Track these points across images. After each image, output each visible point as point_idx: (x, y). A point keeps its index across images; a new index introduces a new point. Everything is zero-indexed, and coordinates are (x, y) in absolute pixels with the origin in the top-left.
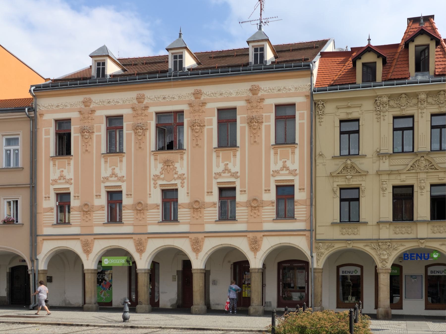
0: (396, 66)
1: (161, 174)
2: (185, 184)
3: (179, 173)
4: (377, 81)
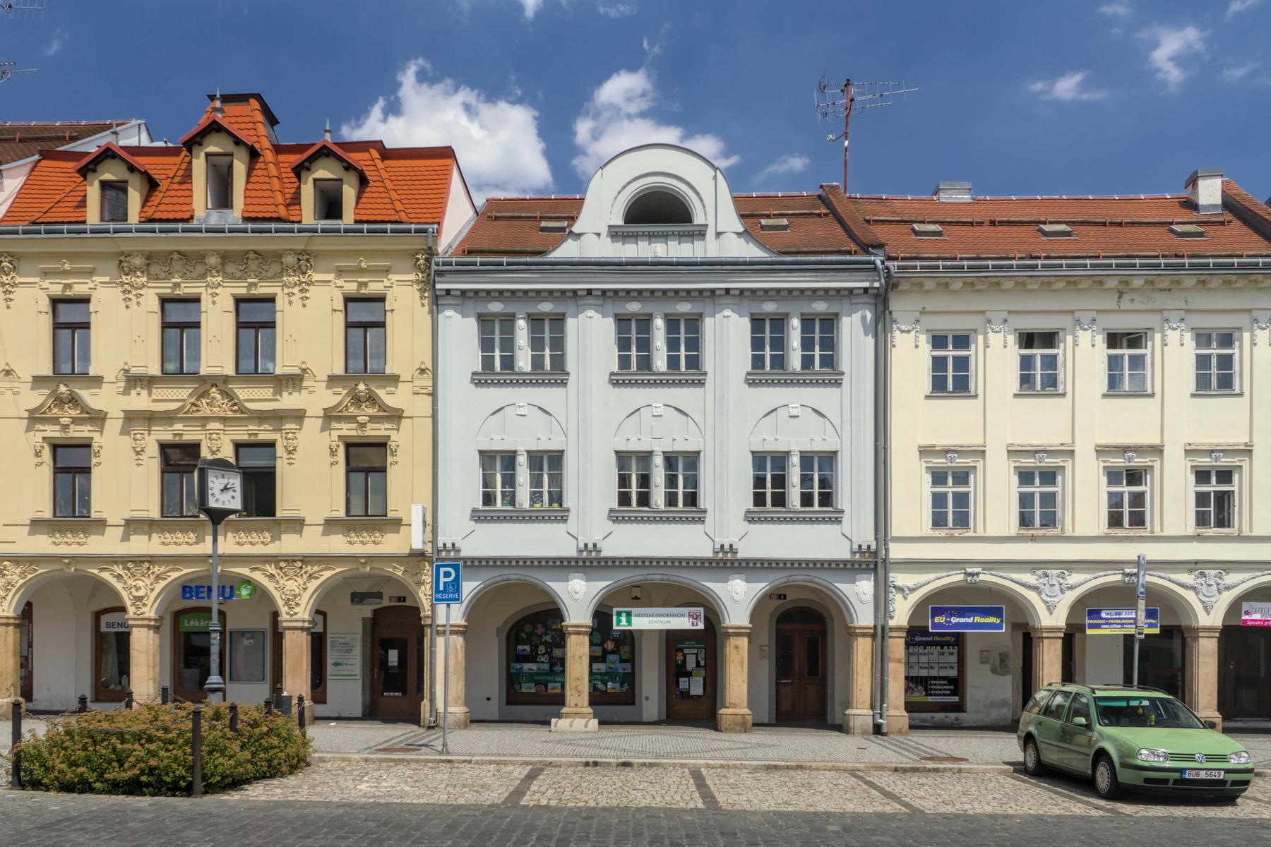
0: (169, 193)
4: (129, 222)
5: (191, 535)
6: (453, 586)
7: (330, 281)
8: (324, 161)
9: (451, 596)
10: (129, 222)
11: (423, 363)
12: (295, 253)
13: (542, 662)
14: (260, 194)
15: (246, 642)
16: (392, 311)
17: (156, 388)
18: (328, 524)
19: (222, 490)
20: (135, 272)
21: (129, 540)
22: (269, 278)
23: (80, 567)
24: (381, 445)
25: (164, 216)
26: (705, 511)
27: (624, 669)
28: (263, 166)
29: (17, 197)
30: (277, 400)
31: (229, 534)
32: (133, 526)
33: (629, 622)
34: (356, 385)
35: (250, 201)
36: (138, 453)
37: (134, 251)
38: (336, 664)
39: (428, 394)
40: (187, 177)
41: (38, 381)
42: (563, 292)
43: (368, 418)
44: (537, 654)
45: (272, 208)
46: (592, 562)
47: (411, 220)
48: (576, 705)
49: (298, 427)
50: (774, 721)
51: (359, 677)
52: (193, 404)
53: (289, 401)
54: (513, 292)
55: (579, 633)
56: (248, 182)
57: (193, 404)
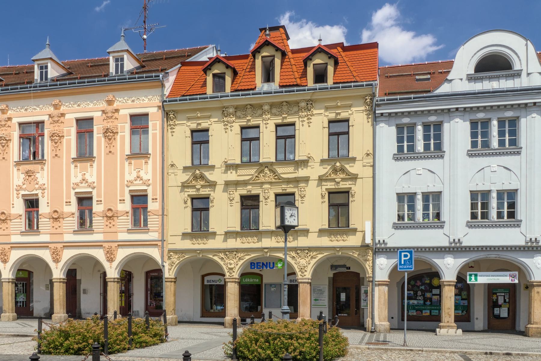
0: (244, 77)
1: (24, 185)
2: (46, 194)
3: (39, 183)
4: (226, 92)
5: (255, 238)
6: (409, 262)
7: (322, 114)
8: (318, 55)
9: (408, 267)
10: (226, 92)
12: (305, 101)
13: (420, 300)
14: (287, 74)
15: (273, 289)
16: (353, 126)
17: (239, 170)
18: (321, 232)
19: (290, 216)
20: (230, 115)
21: (226, 241)
22: (292, 114)
23: (204, 254)
24: (347, 192)
25: (243, 88)
26: (521, 221)
27: (464, 304)
28: (288, 60)
29: (173, 85)
30: (296, 173)
31: (273, 238)
32: (228, 235)
33: (476, 280)
34: (335, 163)
35: (282, 77)
36: (231, 200)
37: (230, 106)
38: (316, 300)
39: (371, 166)
40: (253, 68)
41: (186, 169)
42: (443, 110)
43: (341, 179)
44: (417, 296)
45: (294, 80)
46: (458, 249)
47: (362, 80)
48: (448, 322)
49: (306, 185)
51: (327, 306)
52: (257, 176)
53: (302, 173)
54: (416, 112)
55: (450, 285)
56: (281, 69)
57: (257, 176)
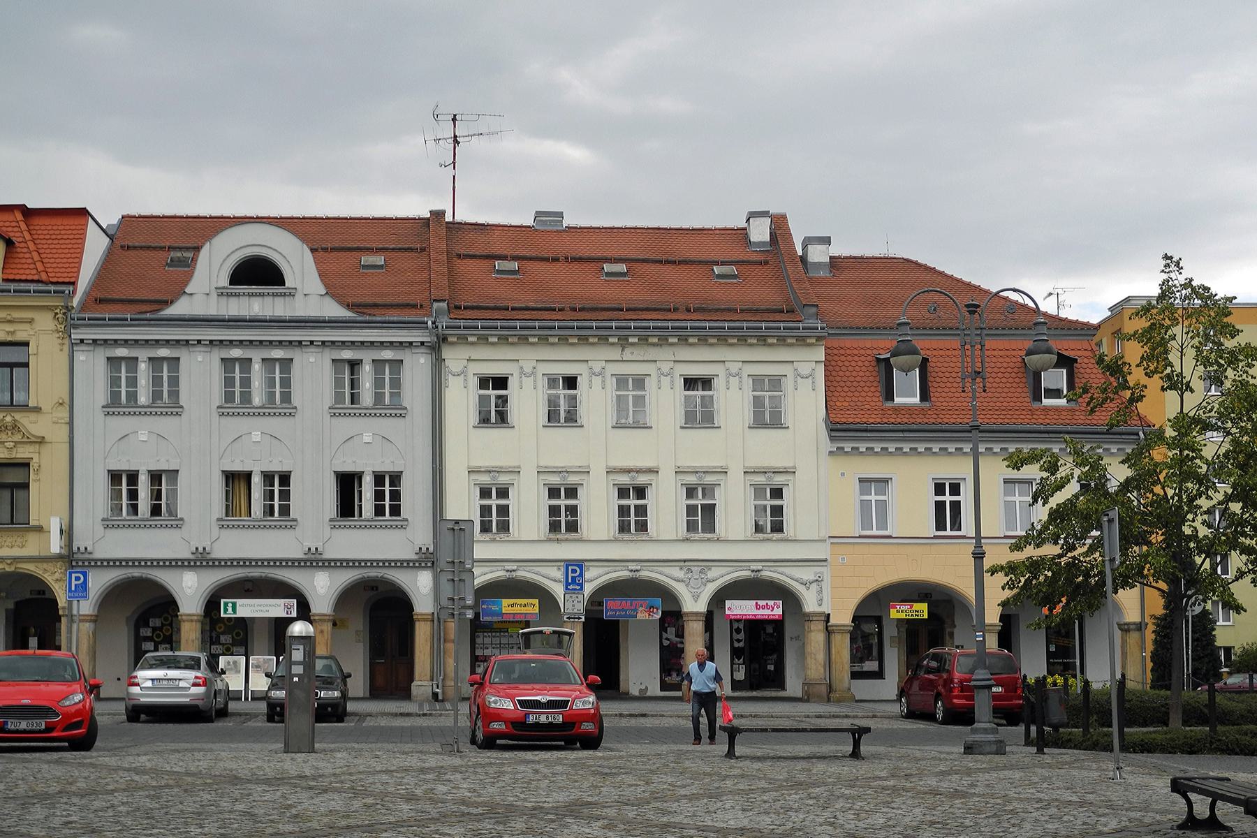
6: (82, 587)
11: (61, 398)
43: (13, 444)
50: (368, 695)
